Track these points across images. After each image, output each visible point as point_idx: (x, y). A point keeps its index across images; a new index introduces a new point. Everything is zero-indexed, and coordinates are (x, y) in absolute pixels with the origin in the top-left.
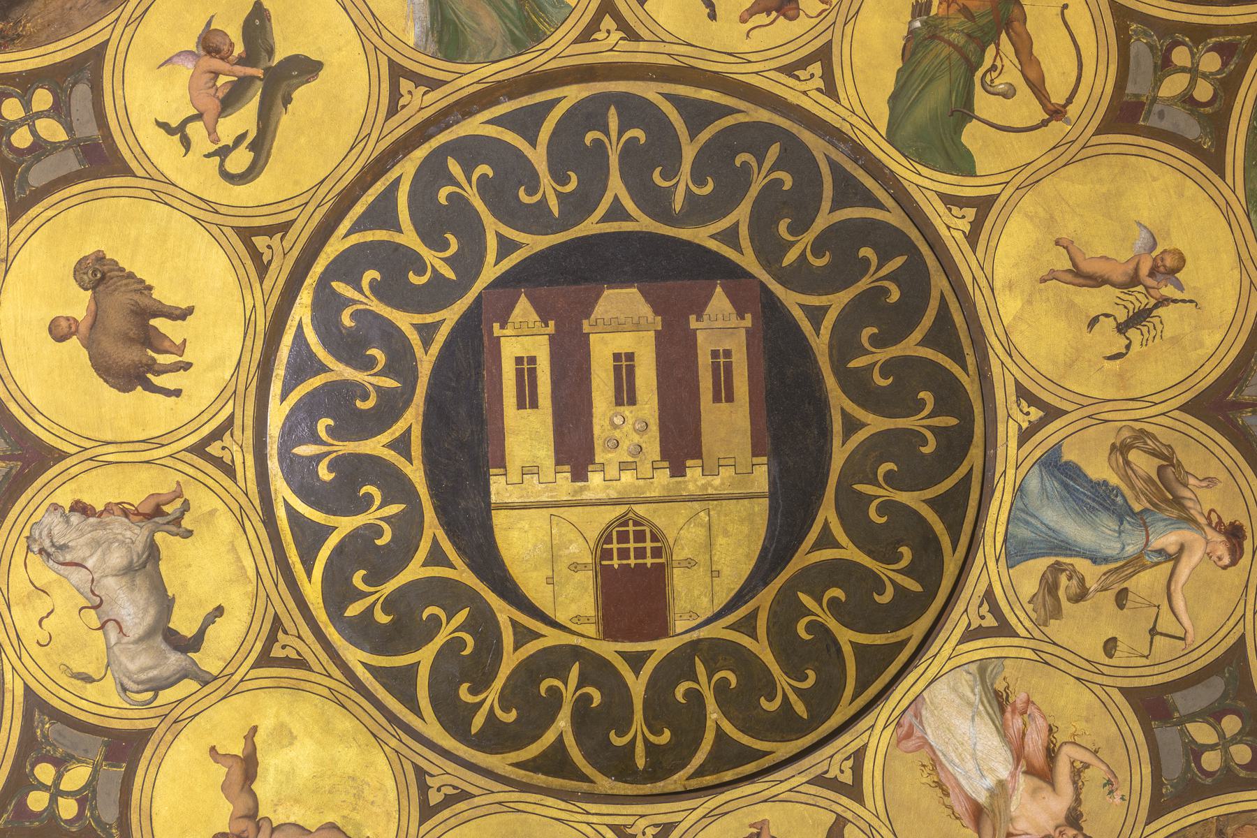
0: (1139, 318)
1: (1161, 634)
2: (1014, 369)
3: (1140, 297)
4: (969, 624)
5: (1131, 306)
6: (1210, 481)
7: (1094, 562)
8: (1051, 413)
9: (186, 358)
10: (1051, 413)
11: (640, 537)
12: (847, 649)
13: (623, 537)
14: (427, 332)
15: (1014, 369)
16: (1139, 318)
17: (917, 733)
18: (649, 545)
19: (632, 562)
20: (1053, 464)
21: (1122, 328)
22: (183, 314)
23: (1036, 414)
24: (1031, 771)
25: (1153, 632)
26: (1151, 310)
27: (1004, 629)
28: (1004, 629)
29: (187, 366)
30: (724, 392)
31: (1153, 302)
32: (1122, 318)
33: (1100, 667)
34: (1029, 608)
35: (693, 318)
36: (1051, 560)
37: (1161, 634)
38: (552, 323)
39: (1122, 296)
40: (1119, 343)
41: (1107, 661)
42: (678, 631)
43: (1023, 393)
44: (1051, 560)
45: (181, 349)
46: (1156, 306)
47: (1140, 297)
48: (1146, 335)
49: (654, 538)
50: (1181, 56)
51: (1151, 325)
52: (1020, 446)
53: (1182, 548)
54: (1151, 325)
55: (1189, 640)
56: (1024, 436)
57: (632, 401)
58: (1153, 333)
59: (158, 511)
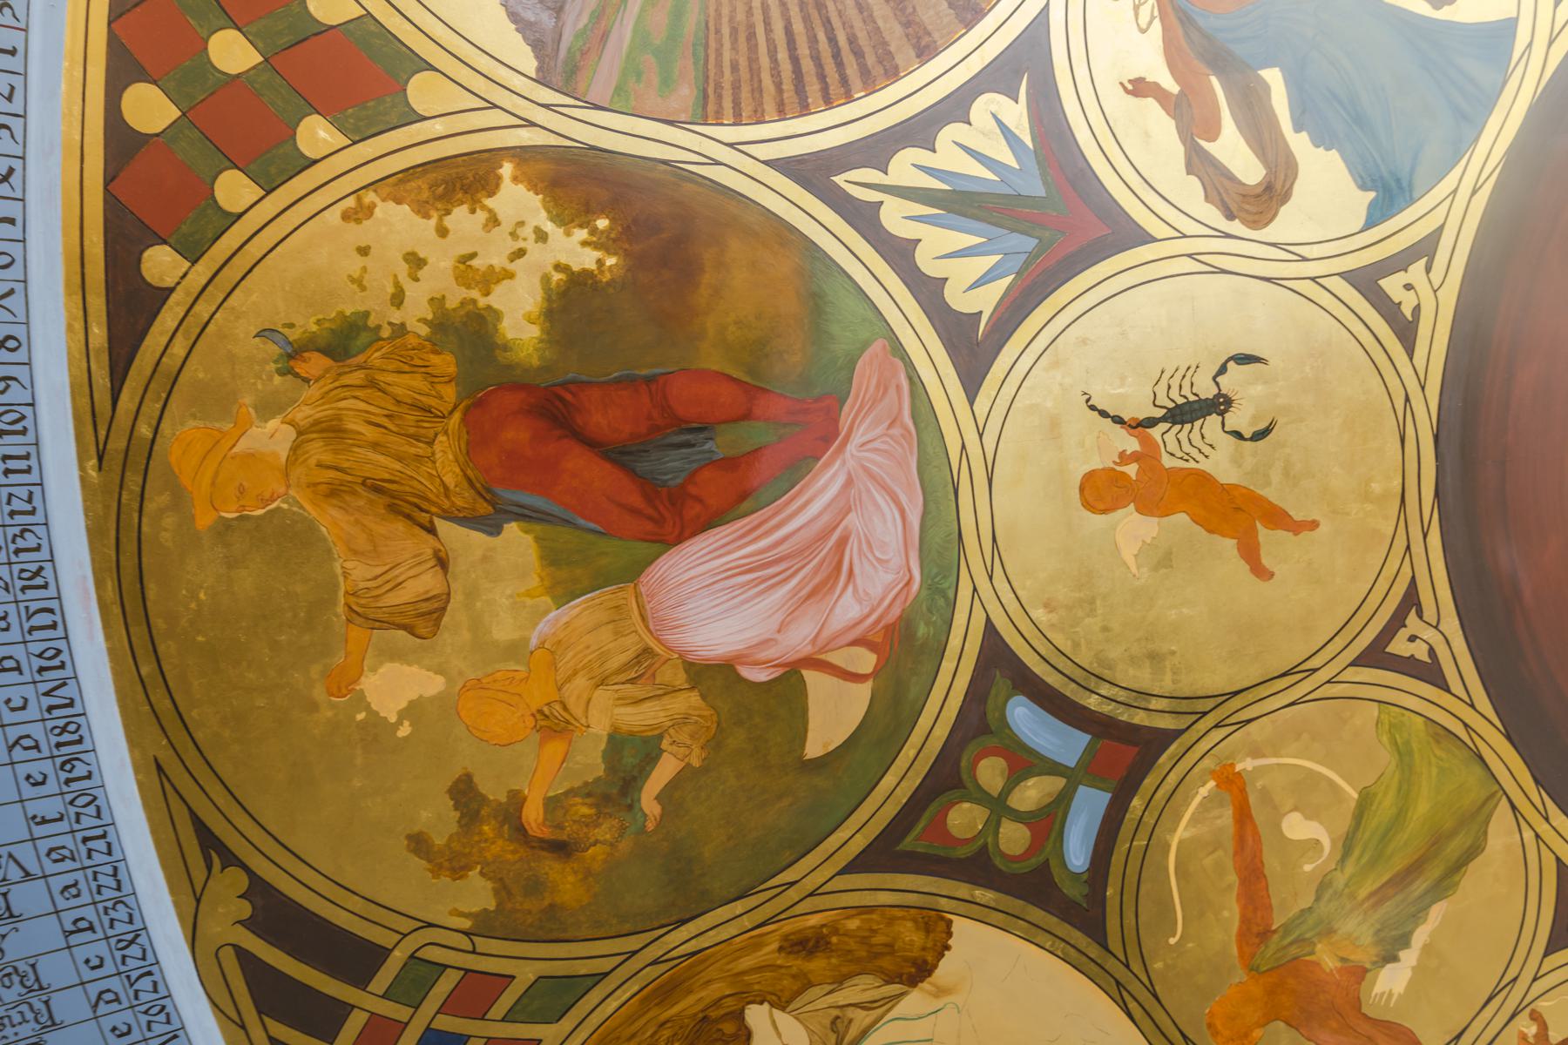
0: (1182, 414)
2: (1407, 371)
3: (1172, 445)
5: (1195, 436)
6: (1139, 88)
8: (1366, 281)
10: (1366, 281)
15: (1407, 371)
16: (1182, 414)
21: (1220, 404)
26: (1163, 419)
31: (1156, 432)
32: (1213, 420)
39: (1200, 457)
46: (1151, 422)
47: (1172, 445)
48: (1186, 383)
50: (1013, 838)
54: (1174, 394)
56: (1425, 249)
58: (1175, 383)
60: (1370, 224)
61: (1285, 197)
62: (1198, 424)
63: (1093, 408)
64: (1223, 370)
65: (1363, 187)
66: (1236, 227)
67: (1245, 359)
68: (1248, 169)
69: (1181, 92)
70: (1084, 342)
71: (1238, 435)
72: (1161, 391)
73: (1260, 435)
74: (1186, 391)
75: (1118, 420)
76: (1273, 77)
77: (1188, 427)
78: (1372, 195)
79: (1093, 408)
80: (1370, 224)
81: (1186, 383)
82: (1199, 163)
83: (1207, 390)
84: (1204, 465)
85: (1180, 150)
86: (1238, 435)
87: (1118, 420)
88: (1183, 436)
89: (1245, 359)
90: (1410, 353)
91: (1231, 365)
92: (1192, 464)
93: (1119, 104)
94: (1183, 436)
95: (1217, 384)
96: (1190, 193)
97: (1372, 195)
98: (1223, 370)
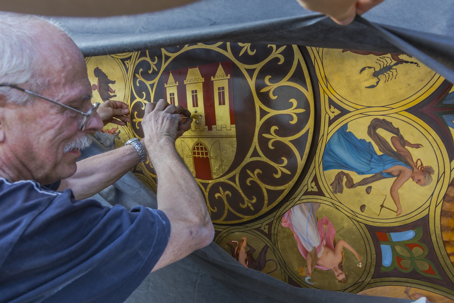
1: (385, 207)
4: (307, 189)
6: (417, 146)
7: (359, 174)
8: (344, 112)
9: (115, 94)
10: (344, 112)
11: (202, 149)
12: (265, 191)
13: (198, 149)
14: (152, 86)
17: (288, 222)
18: (204, 151)
19: (201, 156)
20: (343, 132)
22: (113, 82)
23: (337, 112)
24: (327, 246)
25: (382, 206)
27: (320, 193)
28: (320, 193)
29: (115, 96)
30: (222, 103)
31: (394, 62)
32: (377, 69)
33: (357, 214)
34: (331, 187)
35: (212, 77)
36: (340, 170)
37: (385, 207)
38: (177, 82)
40: (373, 81)
41: (361, 213)
42: (214, 178)
43: (331, 103)
44: (340, 170)
45: (114, 92)
46: (395, 65)
49: (206, 150)
51: (391, 73)
52: (330, 125)
53: (400, 172)
54: (391, 73)
55: (398, 213)
56: (331, 122)
57: (197, 106)
59: (114, 132)
60: (347, 123)
61: (369, 127)
62: (382, 67)
63: (416, 63)
64: (378, 83)
65: (350, 132)
66: (381, 118)
67: (373, 87)
68: (381, 132)
69: (404, 147)
70: (422, 80)
71: (370, 68)
72: (395, 74)
73: (364, 69)
74: (387, 75)
75: (407, 62)
76: (379, 153)
77: (385, 66)
78: (347, 131)
79: (416, 63)
80: (347, 123)
81: (387, 77)
82: (396, 131)
83: (382, 77)
84: (378, 57)
85: (402, 133)
86: (370, 68)
87: (407, 62)
88: (386, 63)
89: (373, 87)
90: (329, 98)
91: (376, 84)
92: (381, 56)
93: (424, 142)
94: (386, 63)
95: (378, 79)
96: (396, 124)
97: (347, 131)
98: (378, 83)
